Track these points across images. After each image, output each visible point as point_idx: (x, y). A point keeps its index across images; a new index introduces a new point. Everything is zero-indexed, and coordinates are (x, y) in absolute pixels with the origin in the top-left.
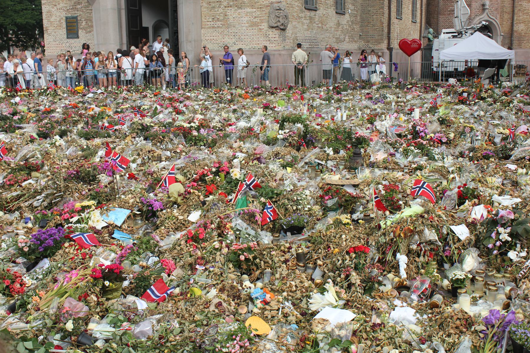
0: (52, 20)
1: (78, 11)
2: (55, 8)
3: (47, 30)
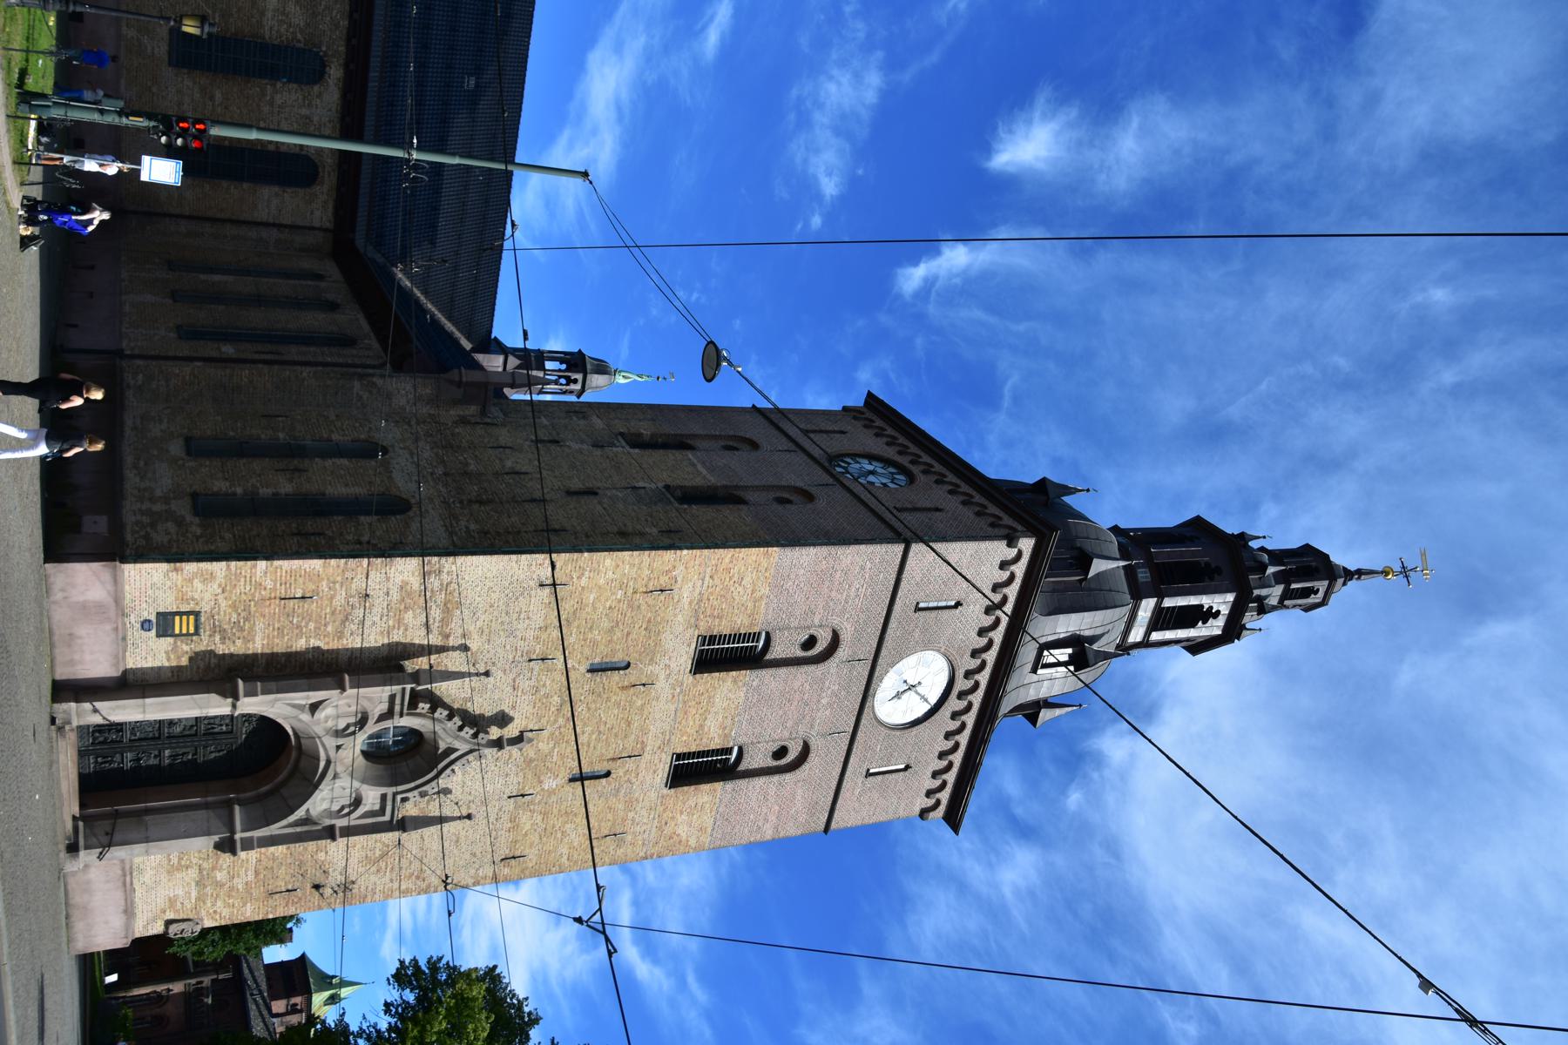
0: (197, 584)
1: (210, 636)
2: (220, 591)
3: (176, 570)
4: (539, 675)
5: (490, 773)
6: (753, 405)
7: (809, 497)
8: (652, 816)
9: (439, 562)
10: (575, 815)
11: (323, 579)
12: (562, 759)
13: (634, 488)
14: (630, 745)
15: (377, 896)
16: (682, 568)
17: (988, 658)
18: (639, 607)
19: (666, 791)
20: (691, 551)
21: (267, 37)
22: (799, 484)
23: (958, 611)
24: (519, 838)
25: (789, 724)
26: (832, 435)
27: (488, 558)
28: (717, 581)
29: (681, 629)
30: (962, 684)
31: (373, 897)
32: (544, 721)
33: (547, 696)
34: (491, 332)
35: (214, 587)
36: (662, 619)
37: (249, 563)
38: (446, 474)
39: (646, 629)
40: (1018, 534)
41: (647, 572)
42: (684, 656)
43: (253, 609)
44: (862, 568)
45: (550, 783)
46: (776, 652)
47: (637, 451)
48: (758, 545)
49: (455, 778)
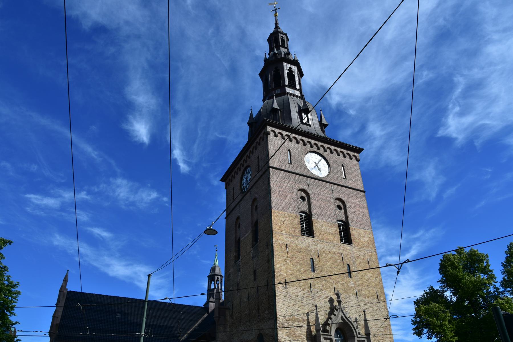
4: (316, 288)
6: (225, 218)
7: (255, 199)
8: (362, 250)
9: (279, 323)
10: (362, 275)
13: (253, 258)
14: (338, 257)
16: (279, 241)
17: (306, 140)
18: (292, 255)
19: (353, 245)
20: (274, 238)
22: (251, 203)
23: (291, 150)
24: (371, 294)
25: (330, 205)
26: (234, 193)
27: (277, 306)
28: (283, 229)
29: (299, 241)
30: (315, 149)
32: (331, 287)
33: (323, 286)
34: (202, 307)
36: (296, 247)
38: (249, 321)
40: (266, 131)
41: (281, 253)
42: (308, 240)
44: (278, 182)
45: (352, 284)
46: (306, 209)
47: (240, 257)
48: (271, 216)
49: (351, 317)
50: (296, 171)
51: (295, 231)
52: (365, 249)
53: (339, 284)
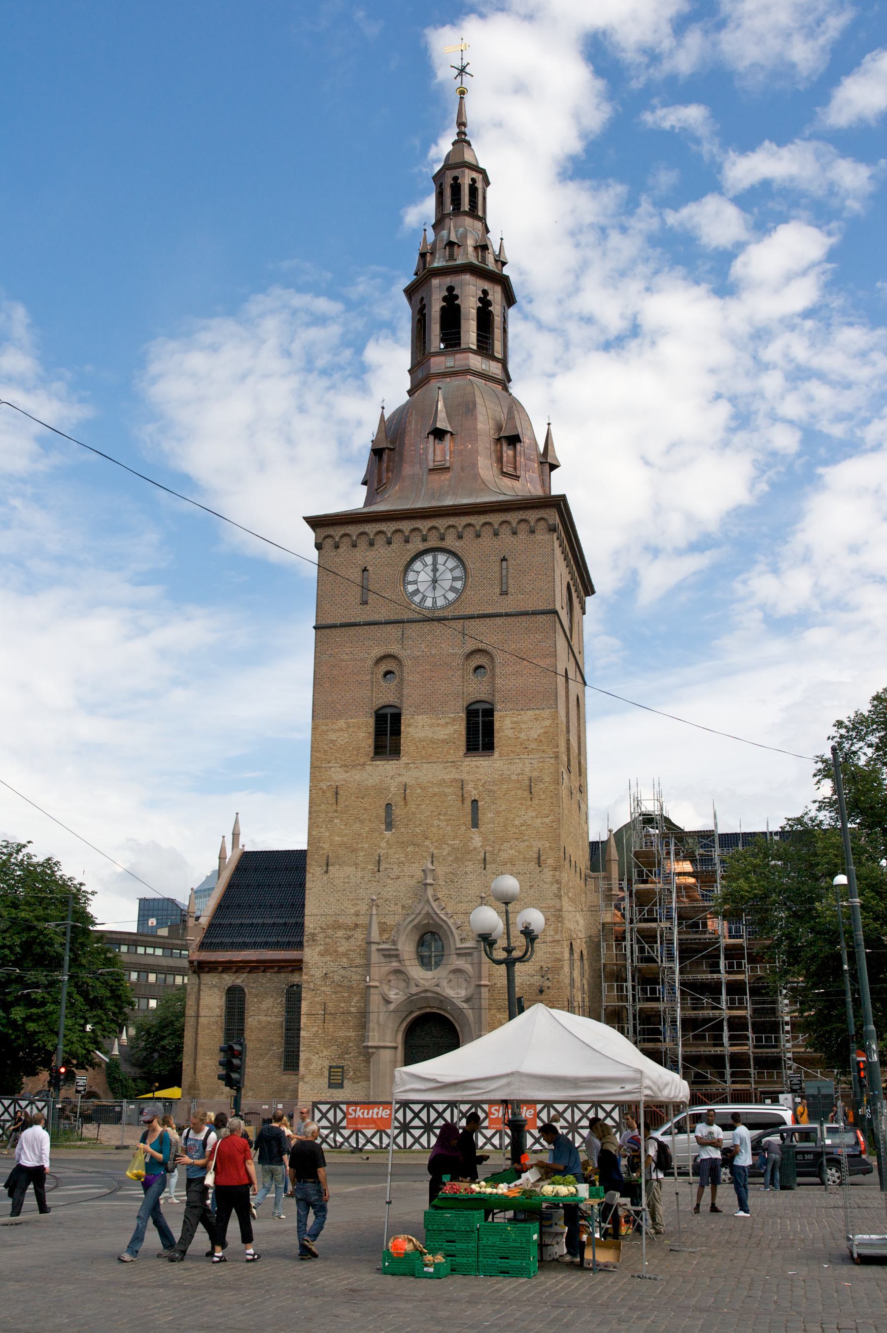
1: (345, 1060)
2: (317, 1056)
3: (303, 1078)
5: (462, 885)
8: (517, 761)
11: (314, 1001)
12: (458, 837)
15: (556, 951)
16: (321, 784)
18: (346, 806)
21: (281, 1019)
24: (521, 856)
31: (557, 953)
32: (425, 854)
35: (315, 1058)
37: (301, 1040)
39: (363, 798)
41: (323, 806)
42: (387, 768)
43: (330, 1038)
44: (331, 656)
45: (477, 841)
50: (376, 618)
51: (357, 755)
52: (527, 757)
53: (444, 846)
